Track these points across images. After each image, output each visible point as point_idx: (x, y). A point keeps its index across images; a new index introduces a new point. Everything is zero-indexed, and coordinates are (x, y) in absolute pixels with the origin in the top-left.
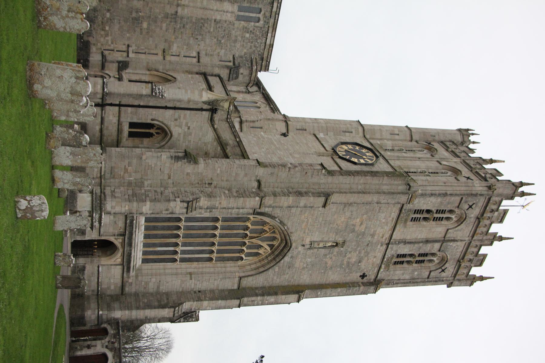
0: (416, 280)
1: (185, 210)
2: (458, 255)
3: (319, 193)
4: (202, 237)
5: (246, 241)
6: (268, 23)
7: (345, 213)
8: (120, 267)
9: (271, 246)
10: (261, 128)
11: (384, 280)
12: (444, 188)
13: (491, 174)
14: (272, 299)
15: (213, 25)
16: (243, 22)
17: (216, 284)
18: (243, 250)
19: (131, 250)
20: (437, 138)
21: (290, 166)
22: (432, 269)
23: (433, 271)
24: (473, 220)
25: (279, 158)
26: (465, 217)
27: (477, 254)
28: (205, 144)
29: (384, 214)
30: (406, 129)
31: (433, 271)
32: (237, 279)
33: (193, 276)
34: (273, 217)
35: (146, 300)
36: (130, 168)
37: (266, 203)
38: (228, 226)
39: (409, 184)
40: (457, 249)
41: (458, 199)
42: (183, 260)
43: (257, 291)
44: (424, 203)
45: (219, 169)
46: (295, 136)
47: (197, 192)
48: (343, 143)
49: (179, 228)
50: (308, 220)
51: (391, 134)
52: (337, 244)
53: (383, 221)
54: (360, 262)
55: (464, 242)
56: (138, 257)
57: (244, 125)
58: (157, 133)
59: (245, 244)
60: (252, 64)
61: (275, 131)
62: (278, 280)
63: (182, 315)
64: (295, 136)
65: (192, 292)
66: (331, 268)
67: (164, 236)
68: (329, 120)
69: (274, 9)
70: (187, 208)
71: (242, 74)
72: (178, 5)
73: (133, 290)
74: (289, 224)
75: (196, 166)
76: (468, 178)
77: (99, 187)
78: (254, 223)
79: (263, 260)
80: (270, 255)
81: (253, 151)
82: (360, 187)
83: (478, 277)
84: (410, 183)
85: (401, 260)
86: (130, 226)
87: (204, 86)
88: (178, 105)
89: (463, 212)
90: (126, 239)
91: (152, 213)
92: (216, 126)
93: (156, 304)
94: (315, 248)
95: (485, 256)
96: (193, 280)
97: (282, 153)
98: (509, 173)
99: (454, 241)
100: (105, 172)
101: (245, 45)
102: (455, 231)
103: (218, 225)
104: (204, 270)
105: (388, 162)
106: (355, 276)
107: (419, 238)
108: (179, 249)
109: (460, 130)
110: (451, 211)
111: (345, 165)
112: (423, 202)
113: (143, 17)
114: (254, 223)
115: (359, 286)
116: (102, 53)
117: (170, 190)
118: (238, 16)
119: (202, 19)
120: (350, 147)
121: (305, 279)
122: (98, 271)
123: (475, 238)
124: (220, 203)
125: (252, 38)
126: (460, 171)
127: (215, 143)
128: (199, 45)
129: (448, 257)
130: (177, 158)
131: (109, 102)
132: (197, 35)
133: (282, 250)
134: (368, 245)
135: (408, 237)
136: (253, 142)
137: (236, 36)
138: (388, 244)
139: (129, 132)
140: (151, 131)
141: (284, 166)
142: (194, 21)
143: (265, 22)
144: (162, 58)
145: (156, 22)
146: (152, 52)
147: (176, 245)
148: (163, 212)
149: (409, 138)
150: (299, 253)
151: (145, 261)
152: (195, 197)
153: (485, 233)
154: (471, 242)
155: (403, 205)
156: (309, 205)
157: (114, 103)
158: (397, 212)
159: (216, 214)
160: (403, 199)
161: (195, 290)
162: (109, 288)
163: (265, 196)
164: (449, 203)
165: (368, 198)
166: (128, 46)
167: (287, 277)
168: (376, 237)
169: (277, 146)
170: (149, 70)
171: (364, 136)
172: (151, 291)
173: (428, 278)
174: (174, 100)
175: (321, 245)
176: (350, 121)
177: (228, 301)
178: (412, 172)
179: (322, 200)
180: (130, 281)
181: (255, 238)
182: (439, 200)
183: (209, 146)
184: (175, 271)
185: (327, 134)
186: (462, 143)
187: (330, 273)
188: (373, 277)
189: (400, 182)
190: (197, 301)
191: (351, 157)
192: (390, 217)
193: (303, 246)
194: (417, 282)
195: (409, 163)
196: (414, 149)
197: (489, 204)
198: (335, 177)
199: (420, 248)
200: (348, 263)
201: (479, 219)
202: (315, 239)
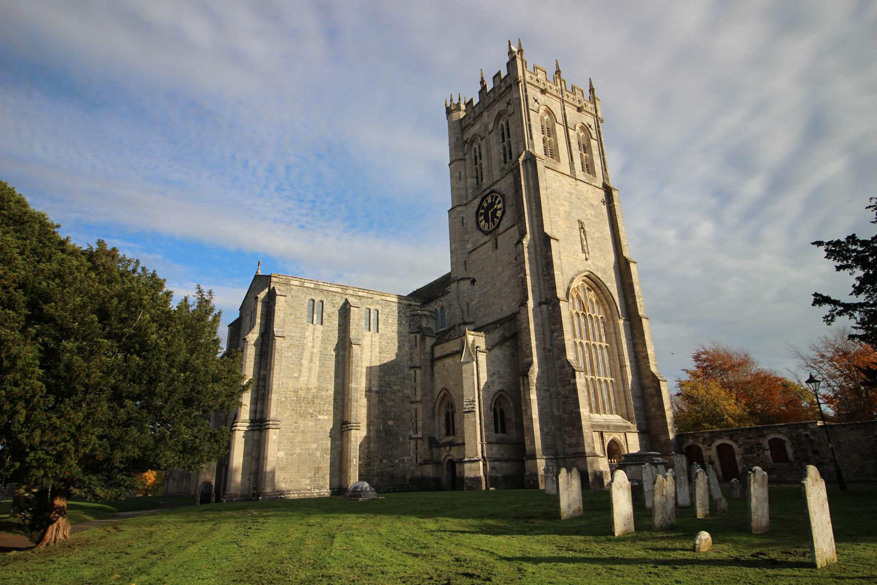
15: (385, 355)
28: (505, 357)
69: (365, 294)
76: (508, 104)
85: (588, 167)
87: (449, 360)
93: (656, 399)
121: (612, 257)
140: (498, 411)
145: (387, 412)
146: (414, 414)
166: (411, 438)
170: (434, 417)
191: (497, 218)
193: (587, 259)
200: (595, 216)
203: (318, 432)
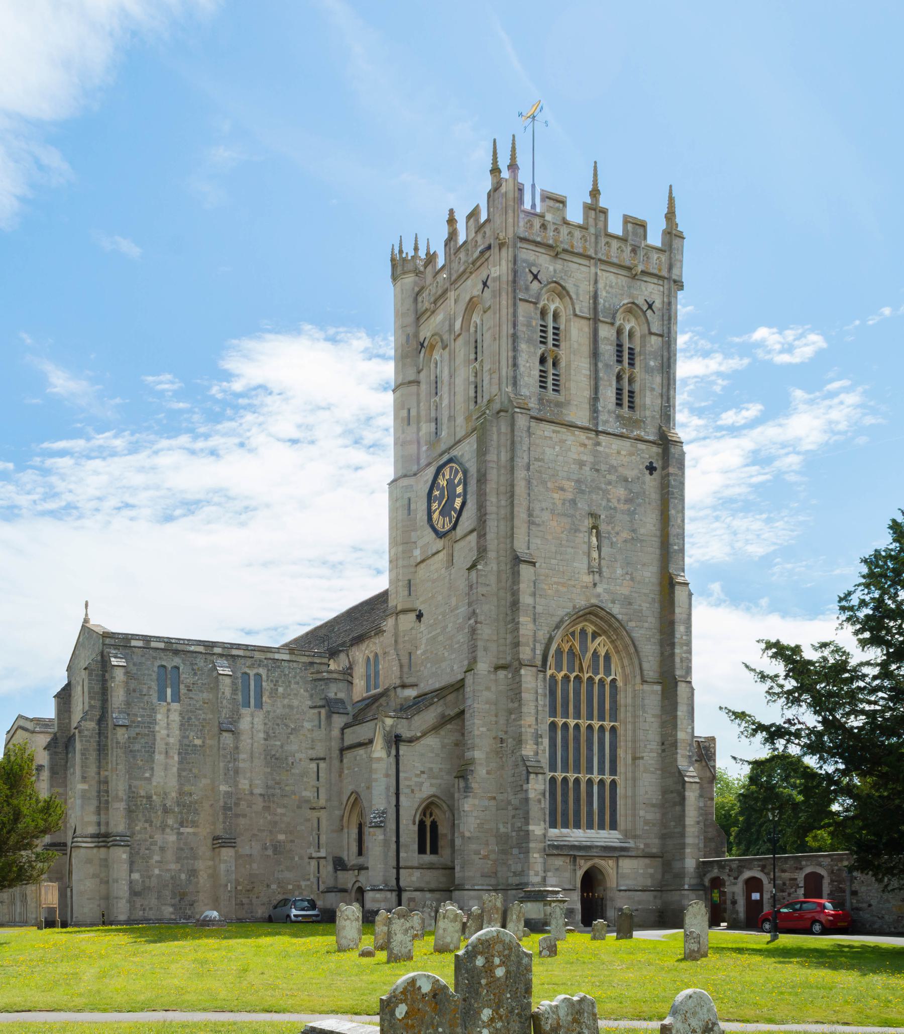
0: (665, 360)
1: (540, 776)
2: (623, 281)
3: (513, 574)
4: (579, 744)
5: (586, 676)
6: (260, 661)
7: (543, 522)
8: (621, 861)
9: (595, 635)
10: (410, 653)
11: (660, 427)
12: (504, 340)
13: (476, 233)
14: (680, 629)
15: (272, 742)
16: (264, 699)
17: (653, 720)
18: (600, 680)
19: (597, 847)
20: (410, 330)
21: (472, 621)
22: (647, 332)
23: (649, 329)
24: (559, 265)
25: (458, 632)
26: (553, 285)
27: (623, 240)
29: (547, 449)
30: (398, 393)
31: (649, 329)
32: (646, 687)
33: (638, 755)
34: (551, 639)
35: (673, 823)
36: (482, 852)
37: (529, 657)
38: (562, 706)
39: (498, 413)
40: (611, 287)
41: (522, 307)
42: (613, 771)
43: (666, 654)
44: (529, 376)
45: (481, 729)
46: (421, 599)
47: (513, 758)
48: (430, 518)
49: (565, 780)
50: (556, 583)
51: (409, 424)
52: (595, 527)
53: (557, 448)
54: (626, 480)
55: (599, 272)
56: (607, 836)
57: (408, 681)
58: (431, 815)
59: (590, 679)
60: (320, 680)
61: (414, 632)
62: (649, 619)
63: (704, 764)
64: (421, 599)
65: (663, 755)
66: (634, 531)
67: (577, 800)
68: (390, 538)
69: (240, 653)
70: (537, 774)
71: (336, 694)
72: (252, 794)
73: (657, 841)
74: (561, 613)
75: (477, 762)
76: (485, 284)
77: (509, 892)
78: (559, 668)
79: (616, 647)
80: (609, 637)
81: (448, 670)
82: (503, 503)
83: (667, 224)
84: (494, 412)
85: (626, 398)
86: (562, 849)
87: (361, 751)
88: (393, 789)
89: (545, 289)
90: (580, 854)
91: (545, 821)
92: (419, 734)
94: (599, 564)
95: (627, 220)
96: (645, 754)
97: (450, 625)
98: (472, 193)
99: (595, 297)
100: (488, 885)
101: (295, 692)
102: (578, 299)
103: (560, 721)
104: (629, 738)
105: (459, 441)
106: (651, 483)
107: (588, 373)
108: (596, 777)
109: (394, 278)
110: (543, 313)
111: (468, 520)
112: (526, 378)
113: (271, 840)
114: (559, 668)
115: (668, 475)
116: (322, 892)
117: (511, 797)
118: (256, 707)
119: (265, 758)
120: (435, 506)
122: (625, 891)
123: (591, 252)
124: (530, 726)
125: (283, 682)
126: (471, 299)
127: (442, 732)
128: (300, 760)
129: (625, 302)
130: (467, 789)
131: (394, 882)
132: (287, 764)
133: (601, 618)
134: (597, 470)
135: (587, 394)
136: (434, 669)
137: (284, 706)
138: (598, 433)
139: (431, 853)
140: (428, 823)
141: (473, 631)
142: (269, 770)
143: (259, 666)
144: (323, 811)
145: (276, 823)
146: (316, 825)
147: (590, 782)
148: (543, 806)
149: (414, 388)
150: (606, 591)
151: (614, 826)
152: (521, 763)
153: (584, 232)
154: (600, 260)
155: (532, 417)
156: (532, 589)
157: (395, 876)
158: (543, 425)
159: (544, 728)
160: (522, 421)
161: (660, 751)
162: (652, 876)
163: (518, 659)
164: (529, 325)
165: (520, 488)
166: (311, 858)
167: (645, 605)
168: (585, 458)
169: (439, 631)
170: (342, 829)
171: (415, 475)
172: (658, 816)
173: (661, 336)
174: (388, 796)
175: (595, 555)
176: (389, 500)
177: (679, 700)
178: (476, 392)
179: (523, 568)
180: (642, 846)
181: (581, 664)
182: (523, 346)
183: (446, 741)
184: (630, 782)
185: (415, 543)
186: (418, 273)
187: (642, 531)
188: (655, 449)
189: (495, 429)
190: (676, 749)
191: (455, 509)
192: (551, 438)
193: (595, 585)
194: (669, 358)
195: (460, 398)
196: (433, 378)
197: (531, 237)
198: (488, 546)
199: (607, 366)
201: (556, 252)
202: (585, 566)
203: (182, 849)
